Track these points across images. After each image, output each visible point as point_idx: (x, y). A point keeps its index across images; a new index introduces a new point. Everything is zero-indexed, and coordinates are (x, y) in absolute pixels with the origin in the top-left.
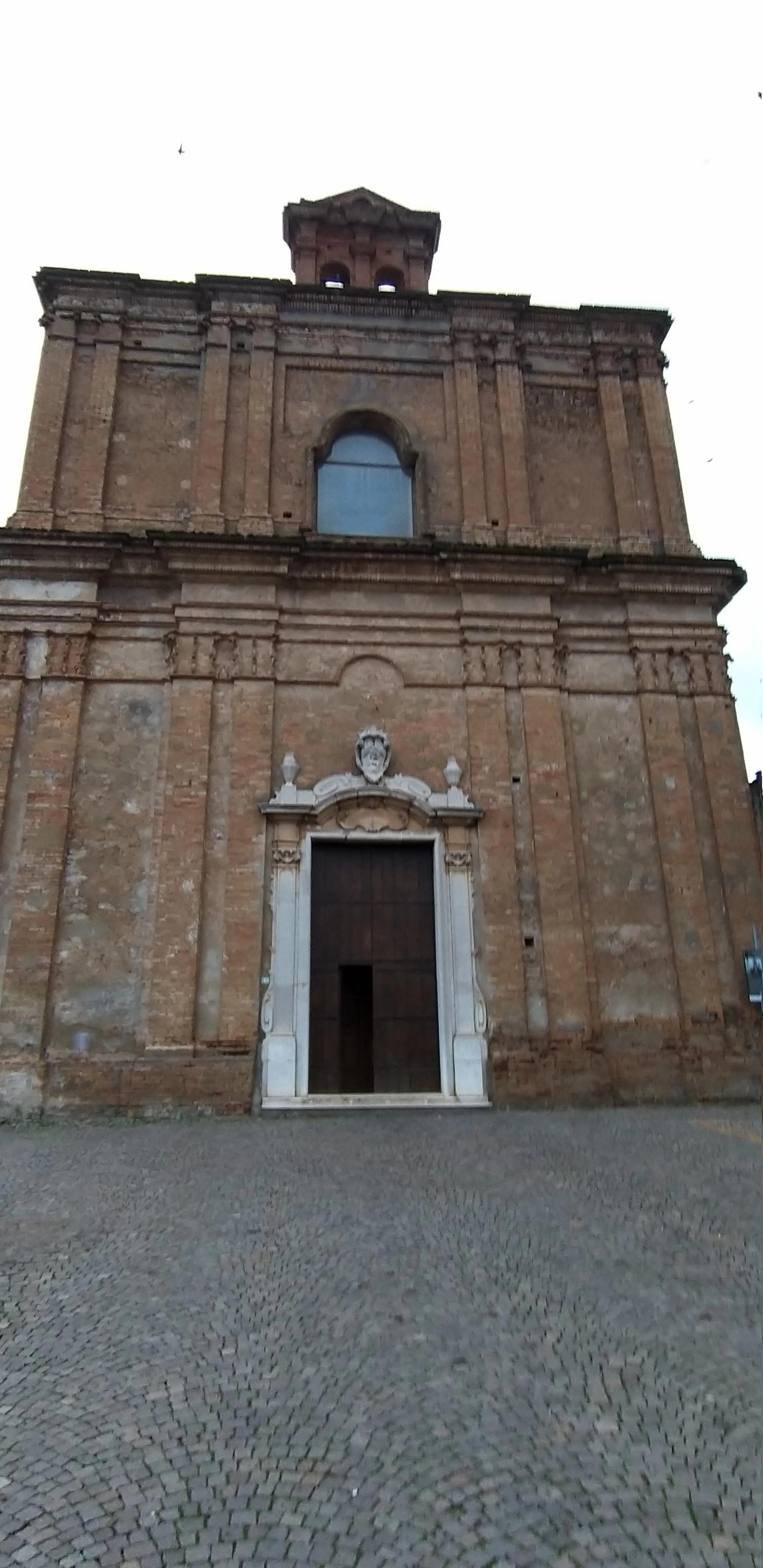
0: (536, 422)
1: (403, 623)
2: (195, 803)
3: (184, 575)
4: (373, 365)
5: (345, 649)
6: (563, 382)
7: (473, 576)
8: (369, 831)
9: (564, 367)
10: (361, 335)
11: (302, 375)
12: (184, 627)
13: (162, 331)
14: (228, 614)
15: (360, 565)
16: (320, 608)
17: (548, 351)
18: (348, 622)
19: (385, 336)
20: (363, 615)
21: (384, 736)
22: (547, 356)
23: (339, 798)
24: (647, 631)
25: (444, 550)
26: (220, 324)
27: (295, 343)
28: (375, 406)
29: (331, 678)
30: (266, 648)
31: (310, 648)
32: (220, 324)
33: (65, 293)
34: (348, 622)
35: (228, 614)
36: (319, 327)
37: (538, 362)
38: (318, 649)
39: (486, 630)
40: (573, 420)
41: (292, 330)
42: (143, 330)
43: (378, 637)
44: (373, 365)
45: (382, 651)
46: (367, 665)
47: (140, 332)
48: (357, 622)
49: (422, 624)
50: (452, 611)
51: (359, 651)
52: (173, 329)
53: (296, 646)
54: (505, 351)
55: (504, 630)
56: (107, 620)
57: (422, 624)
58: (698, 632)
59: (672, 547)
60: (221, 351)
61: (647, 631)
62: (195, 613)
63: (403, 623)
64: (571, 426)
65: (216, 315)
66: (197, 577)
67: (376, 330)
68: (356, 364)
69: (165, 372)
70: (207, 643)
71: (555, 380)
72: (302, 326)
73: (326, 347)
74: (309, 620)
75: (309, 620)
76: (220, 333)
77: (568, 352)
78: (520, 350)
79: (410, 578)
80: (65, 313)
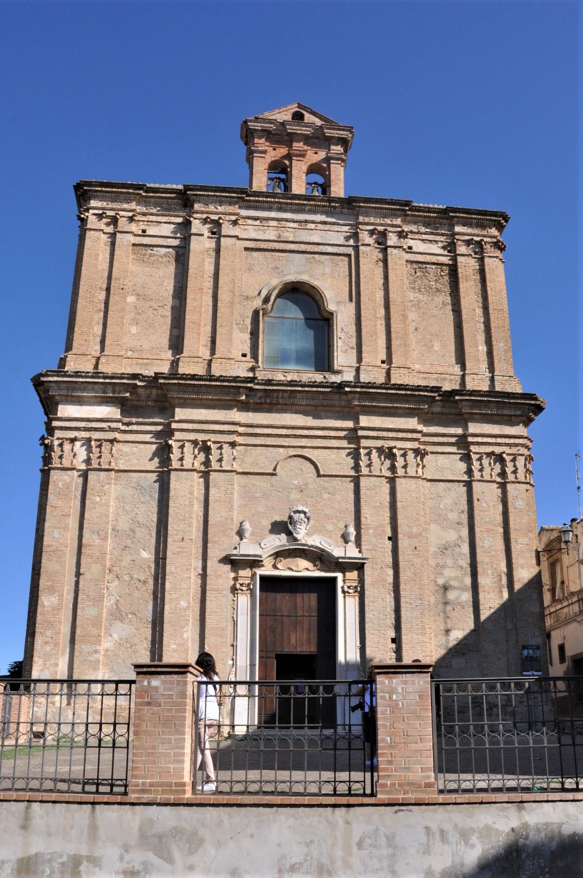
0: (414, 288)
2: (186, 552)
3: (177, 401)
4: (303, 247)
5: (281, 450)
6: (434, 259)
8: (296, 571)
13: (160, 222)
16: (265, 422)
17: (425, 237)
19: (312, 226)
21: (306, 510)
23: (277, 550)
24: (479, 440)
25: (349, 386)
27: (250, 231)
28: (304, 278)
33: (95, 198)
36: (267, 219)
39: (373, 438)
40: (439, 286)
41: (250, 222)
42: (148, 221)
47: (146, 223)
48: (290, 432)
51: (292, 452)
52: (168, 221)
53: (249, 448)
54: (392, 240)
56: (127, 429)
58: (512, 441)
61: (479, 440)
63: (320, 433)
64: (438, 290)
65: (197, 212)
67: (306, 222)
71: (428, 258)
72: (256, 219)
73: (271, 235)
77: (438, 238)
80: (96, 212)
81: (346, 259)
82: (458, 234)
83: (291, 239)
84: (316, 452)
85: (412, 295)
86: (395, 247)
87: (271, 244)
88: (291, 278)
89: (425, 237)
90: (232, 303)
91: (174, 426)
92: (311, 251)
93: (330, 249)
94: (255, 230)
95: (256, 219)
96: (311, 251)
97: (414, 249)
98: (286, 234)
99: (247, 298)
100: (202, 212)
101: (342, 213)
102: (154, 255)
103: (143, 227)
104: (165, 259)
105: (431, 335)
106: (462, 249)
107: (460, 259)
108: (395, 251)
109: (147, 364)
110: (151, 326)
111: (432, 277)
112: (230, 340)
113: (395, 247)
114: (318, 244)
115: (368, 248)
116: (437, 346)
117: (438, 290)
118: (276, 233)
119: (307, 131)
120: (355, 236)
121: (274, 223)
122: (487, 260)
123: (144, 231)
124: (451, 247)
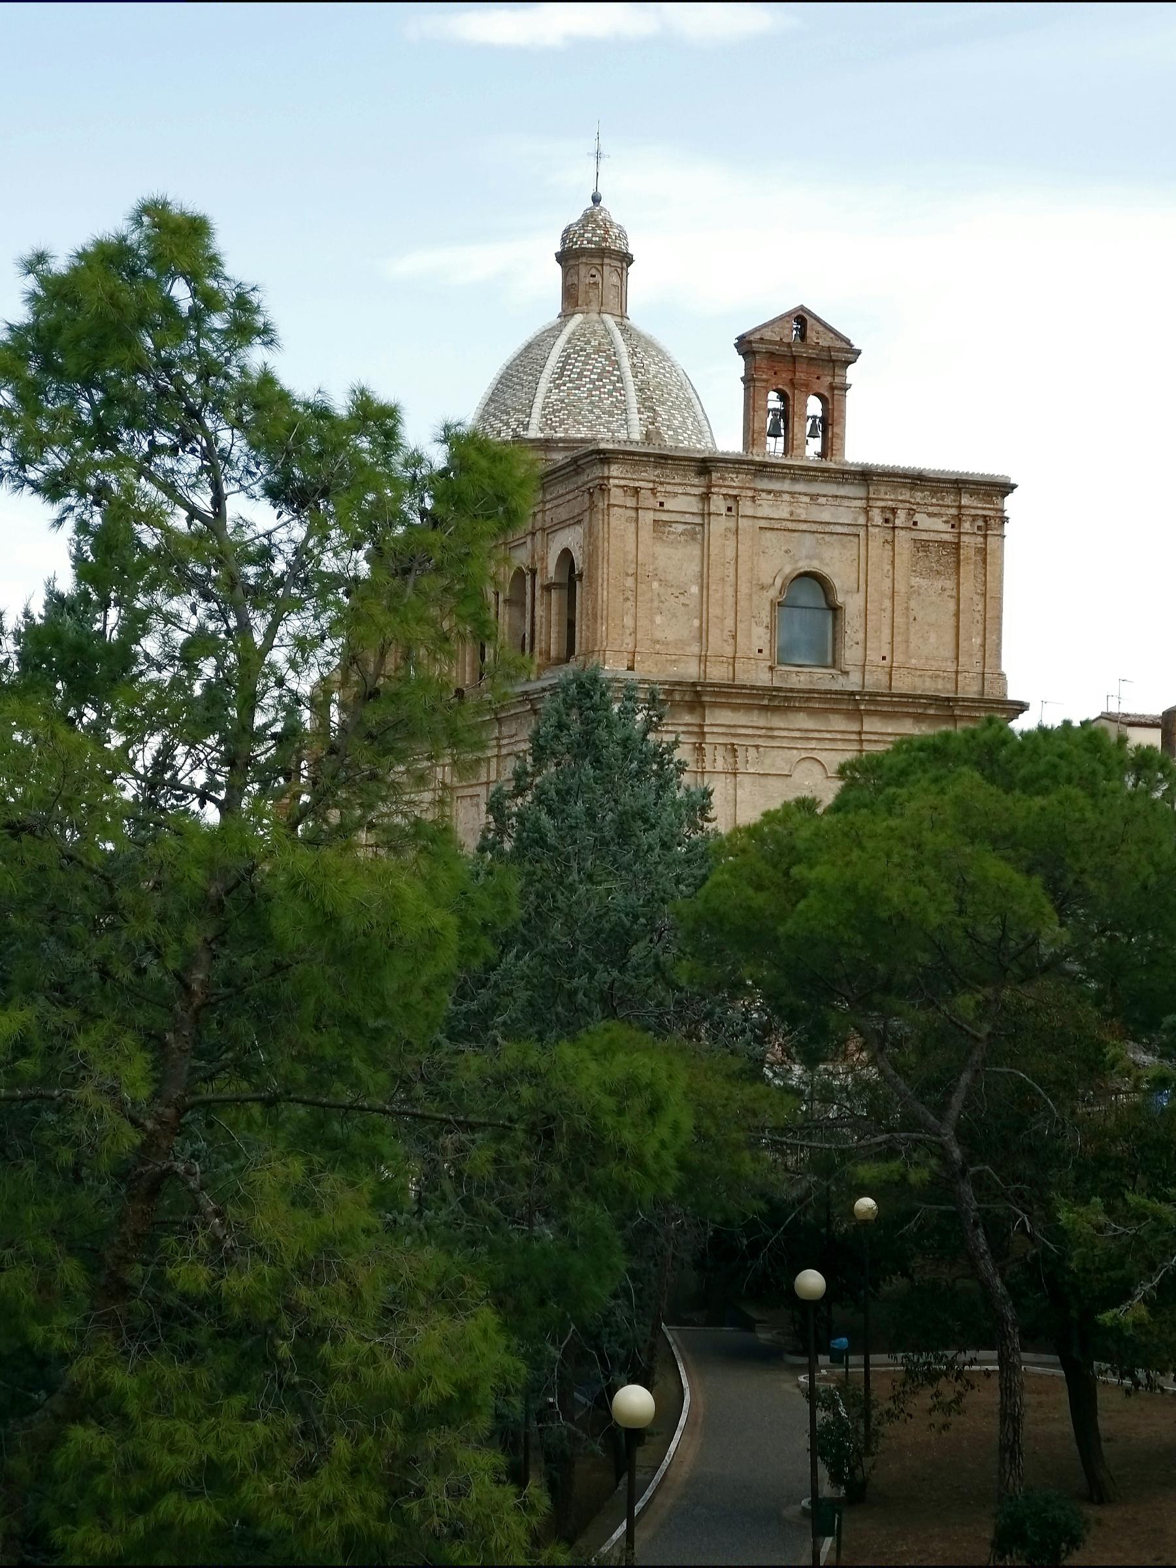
1: (828, 736)
4: (814, 527)
5: (795, 752)
6: (938, 537)
7: (872, 708)
9: (939, 524)
10: (806, 499)
11: (769, 534)
12: (709, 738)
14: (733, 731)
15: (808, 699)
17: (931, 509)
18: (797, 734)
20: (807, 731)
22: (930, 515)
26: (718, 494)
27: (767, 508)
29: (786, 773)
30: (752, 751)
31: (775, 752)
32: (718, 494)
34: (797, 734)
35: (733, 731)
37: (923, 520)
38: (780, 752)
41: (764, 495)
43: (813, 745)
44: (814, 527)
45: (814, 754)
46: (807, 765)
49: (839, 736)
50: (856, 728)
55: (885, 742)
57: (839, 736)
59: (991, 693)
60: (720, 518)
62: (715, 729)
63: (828, 736)
64: (938, 572)
65: (716, 486)
66: (715, 705)
68: (804, 527)
69: (681, 528)
70: (721, 749)
72: (769, 492)
74: (776, 733)
75: (776, 733)
76: (718, 504)
77: (943, 510)
78: (911, 513)
79: (835, 707)
81: (856, 540)
82: (965, 507)
83: (803, 517)
84: (824, 754)
85: (915, 581)
86: (902, 528)
87: (784, 523)
88: (804, 566)
89: (931, 509)
90: (751, 595)
91: (706, 729)
92: (823, 530)
93: (840, 529)
94: (770, 506)
95: (769, 492)
96: (823, 530)
97: (920, 526)
98: (799, 511)
99: (763, 588)
100: (721, 486)
101: (852, 484)
102: (674, 533)
103: (661, 499)
104: (683, 538)
105: (929, 625)
106: (966, 526)
107: (964, 538)
108: (902, 533)
109: (675, 661)
110: (674, 616)
111: (933, 557)
112: (749, 636)
113: (902, 528)
114: (829, 523)
115: (877, 530)
116: (933, 638)
117: (938, 572)
118: (789, 509)
119: (812, 353)
120: (866, 511)
121: (786, 497)
122: (989, 539)
123: (662, 504)
124: (956, 522)
